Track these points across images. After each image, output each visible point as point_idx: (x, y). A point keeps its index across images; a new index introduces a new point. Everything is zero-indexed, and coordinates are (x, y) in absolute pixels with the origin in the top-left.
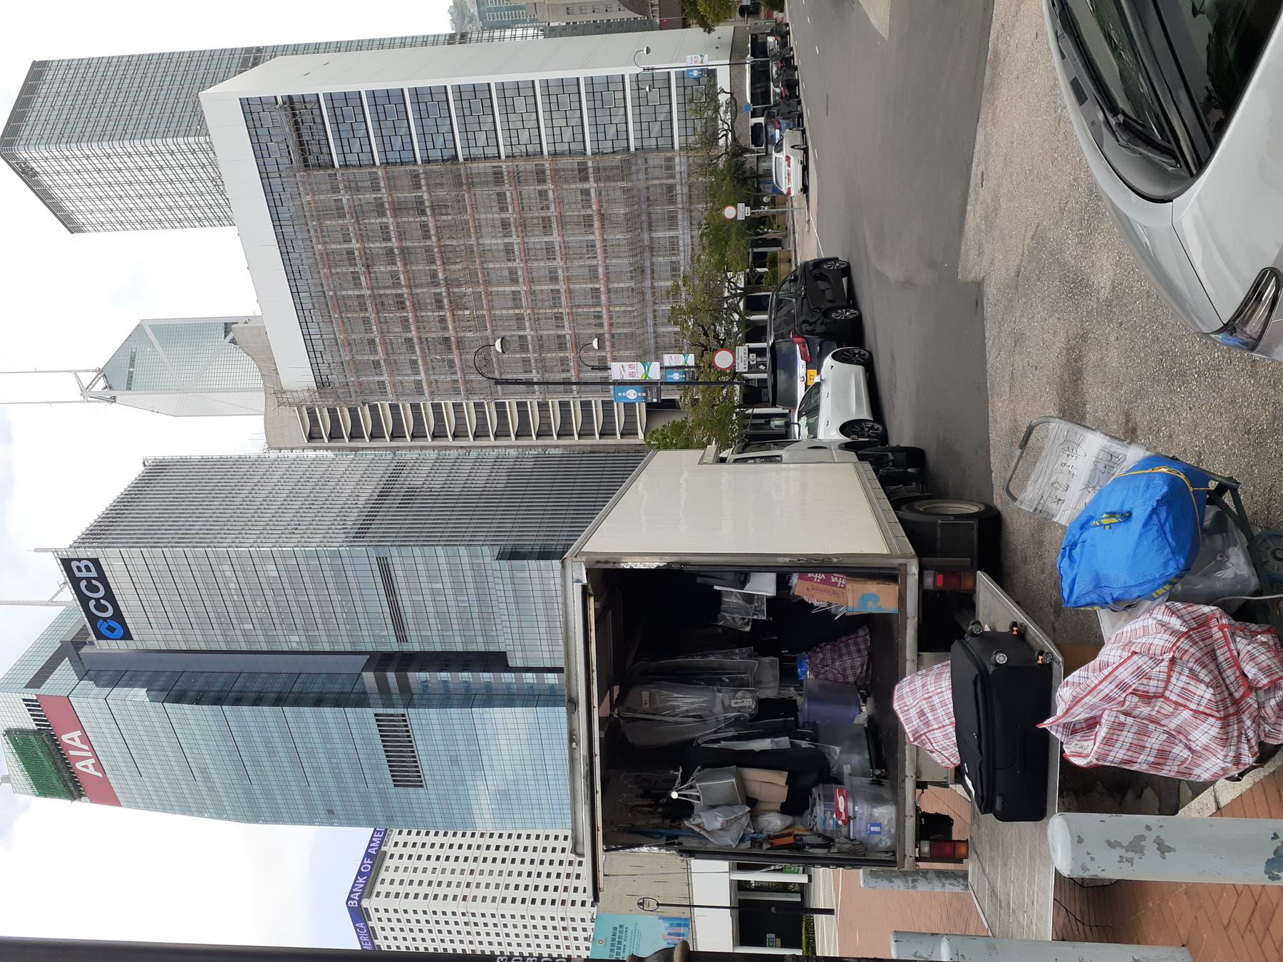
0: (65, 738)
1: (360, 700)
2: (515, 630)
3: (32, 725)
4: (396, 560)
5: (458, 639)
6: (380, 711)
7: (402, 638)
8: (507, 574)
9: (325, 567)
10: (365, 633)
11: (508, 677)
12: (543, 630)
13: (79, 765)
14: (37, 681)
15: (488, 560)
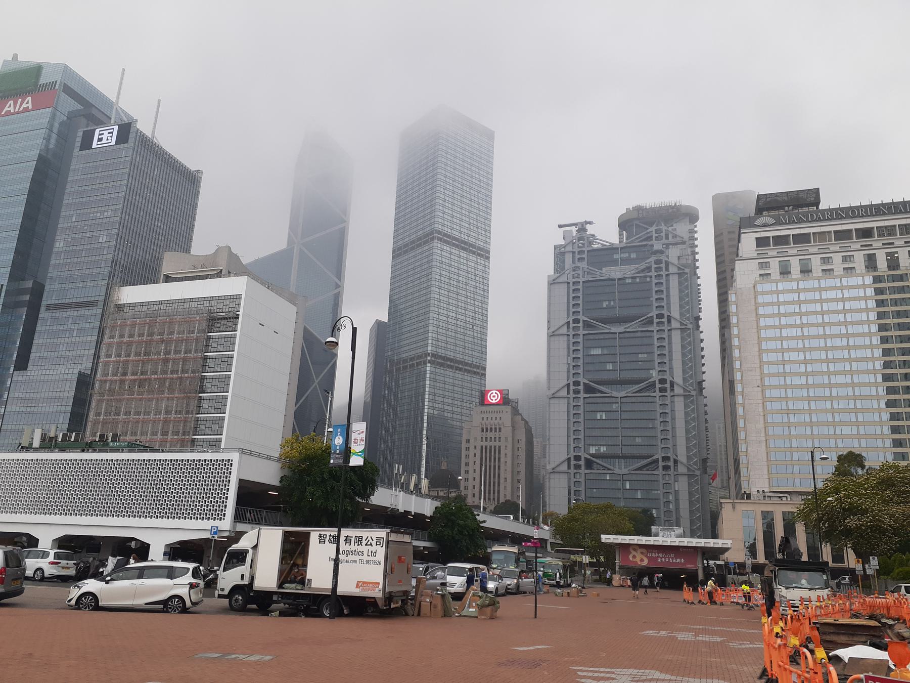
0: (29, 99)
1: (13, 277)
2: (35, 378)
3: (42, 81)
4: (94, 312)
5: (41, 341)
6: (4, 288)
7: (48, 308)
8: (69, 376)
9: (98, 270)
10: (56, 286)
11: (12, 369)
12: (31, 395)
13: (11, 102)
14: (67, 90)
15: (84, 366)
